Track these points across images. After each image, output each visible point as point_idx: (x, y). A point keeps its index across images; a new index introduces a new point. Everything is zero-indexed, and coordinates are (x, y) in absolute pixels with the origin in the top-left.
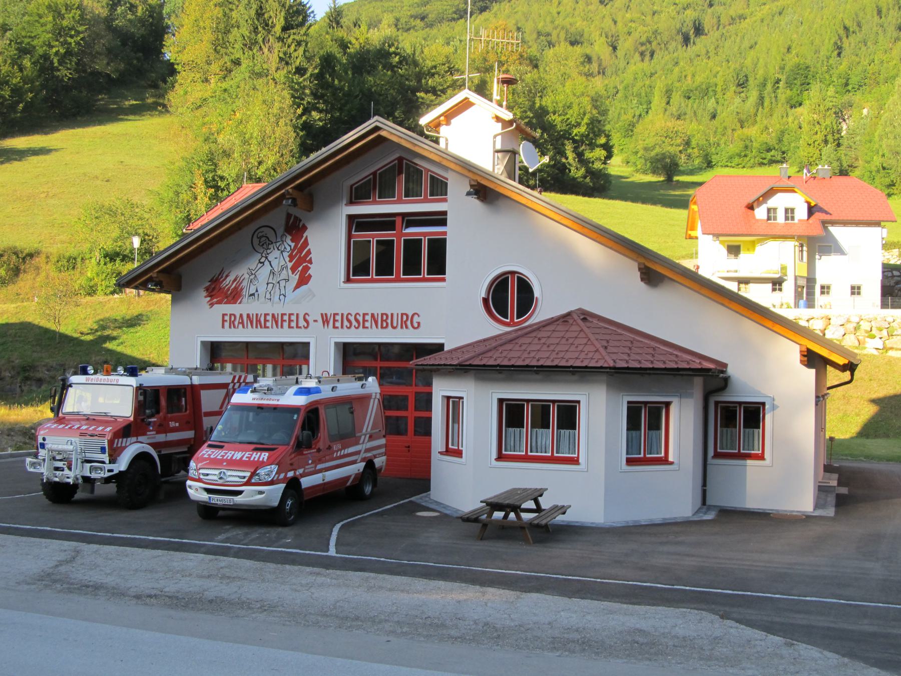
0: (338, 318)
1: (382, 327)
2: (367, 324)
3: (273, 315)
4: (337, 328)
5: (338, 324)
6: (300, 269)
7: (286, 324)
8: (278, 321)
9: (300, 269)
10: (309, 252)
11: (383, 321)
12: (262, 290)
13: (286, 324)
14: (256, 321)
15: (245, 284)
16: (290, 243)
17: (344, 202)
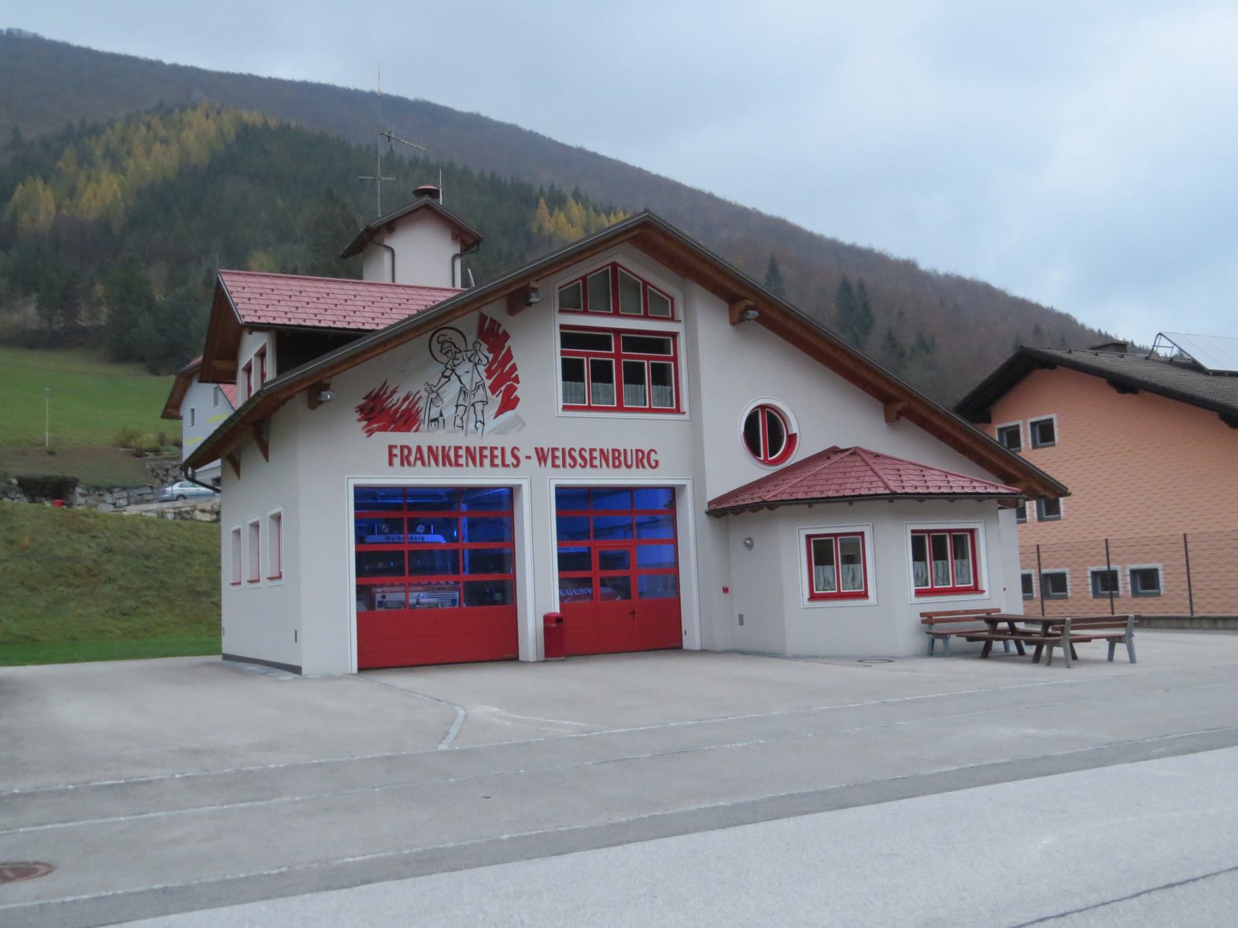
0: (559, 454)
1: (614, 466)
2: (596, 462)
3: (468, 449)
4: (558, 466)
5: (559, 462)
6: (503, 388)
7: (487, 462)
8: (475, 456)
9: (503, 388)
10: (514, 368)
11: (614, 458)
12: (449, 413)
13: (487, 462)
14: (443, 457)
15: (421, 404)
16: (487, 353)
17: (557, 308)
